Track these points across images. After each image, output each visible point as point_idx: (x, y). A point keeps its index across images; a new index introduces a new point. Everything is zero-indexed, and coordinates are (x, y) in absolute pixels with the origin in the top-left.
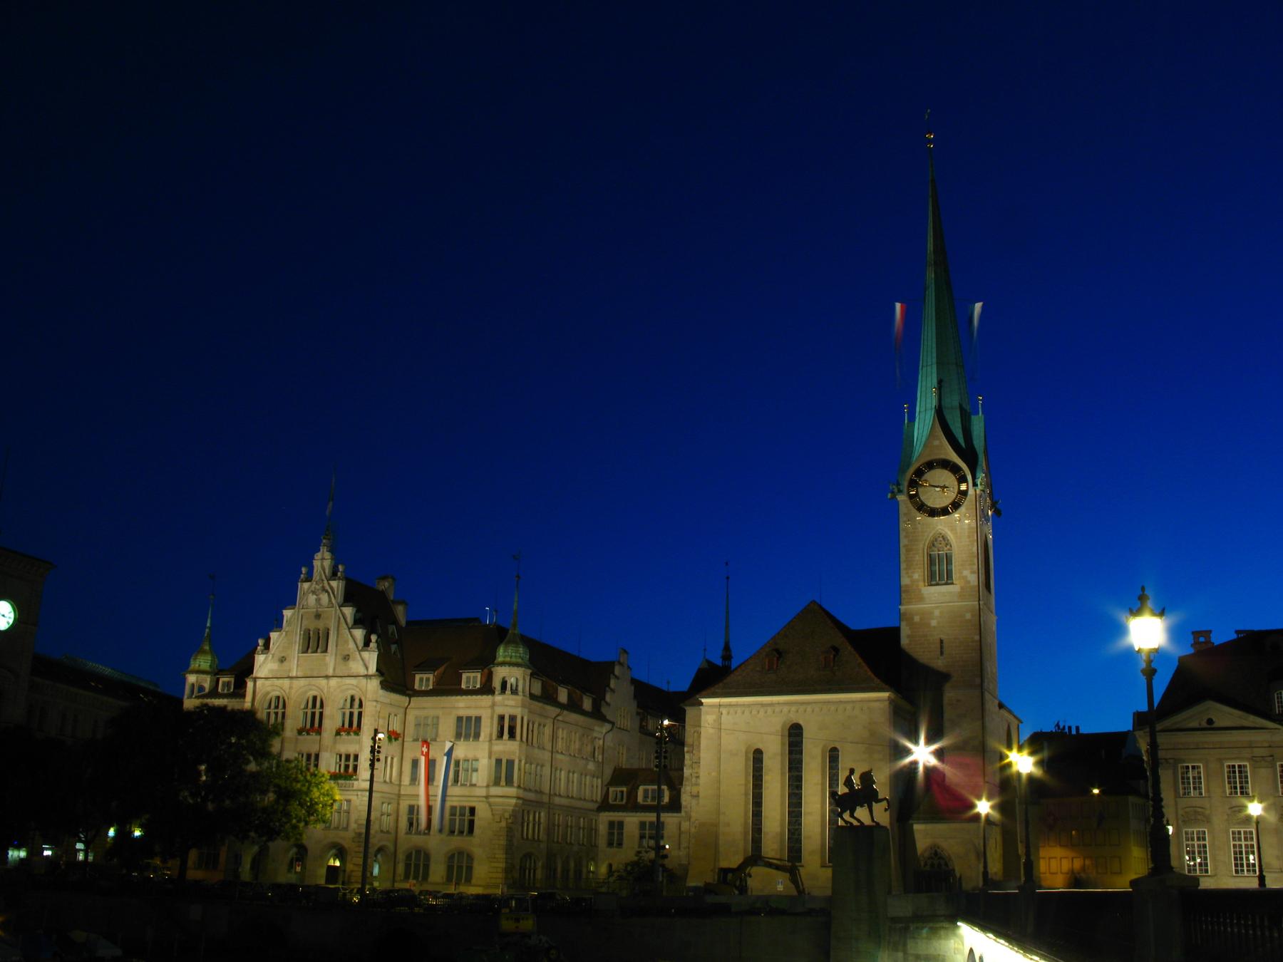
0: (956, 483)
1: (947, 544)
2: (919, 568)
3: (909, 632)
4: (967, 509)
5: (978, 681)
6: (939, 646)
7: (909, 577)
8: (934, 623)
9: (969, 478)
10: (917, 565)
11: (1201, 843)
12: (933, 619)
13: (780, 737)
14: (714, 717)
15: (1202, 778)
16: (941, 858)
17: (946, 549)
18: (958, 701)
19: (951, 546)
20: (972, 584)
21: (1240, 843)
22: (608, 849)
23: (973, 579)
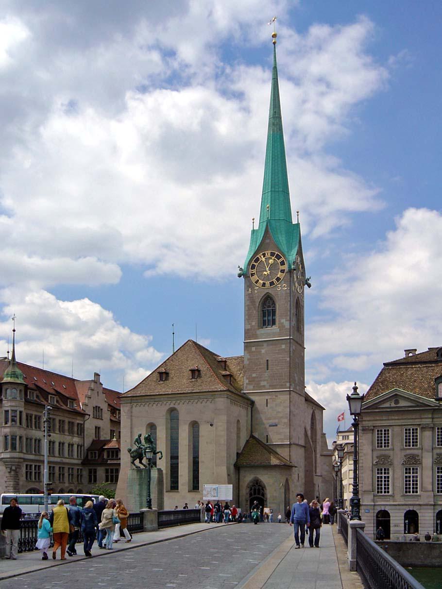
1: (273, 303)
2: (255, 319)
3: (249, 357)
5: (288, 385)
6: (266, 364)
7: (249, 324)
8: (263, 351)
10: (254, 317)
11: (408, 475)
12: (263, 349)
13: (165, 420)
14: (128, 408)
15: (418, 439)
17: (272, 306)
19: (275, 305)
20: (286, 327)
21: (410, 475)
22: (89, 485)
23: (287, 324)
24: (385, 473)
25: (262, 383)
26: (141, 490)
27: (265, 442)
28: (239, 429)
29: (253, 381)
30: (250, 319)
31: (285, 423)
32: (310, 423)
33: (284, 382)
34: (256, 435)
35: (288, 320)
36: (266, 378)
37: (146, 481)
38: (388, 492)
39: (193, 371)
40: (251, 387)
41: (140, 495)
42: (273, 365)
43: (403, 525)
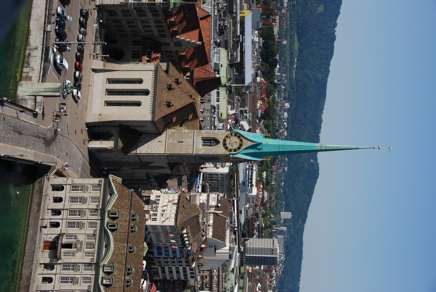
0: (234, 148)
3: (186, 132)
4: (225, 151)
5: (168, 153)
8: (188, 140)
9: (235, 153)
16: (110, 137)
18: (163, 146)
23: (201, 153)
24: (80, 189)
25: (171, 139)
26: (52, 89)
27: (139, 140)
28: (142, 127)
29: (173, 134)
30: (207, 133)
31: (148, 151)
32: (158, 165)
33: (170, 150)
34: (143, 136)
35: (203, 153)
36: (173, 142)
37: (55, 91)
38: (72, 191)
39: (170, 103)
40: (170, 133)
41: (49, 88)
42: (180, 145)
43: (57, 196)
